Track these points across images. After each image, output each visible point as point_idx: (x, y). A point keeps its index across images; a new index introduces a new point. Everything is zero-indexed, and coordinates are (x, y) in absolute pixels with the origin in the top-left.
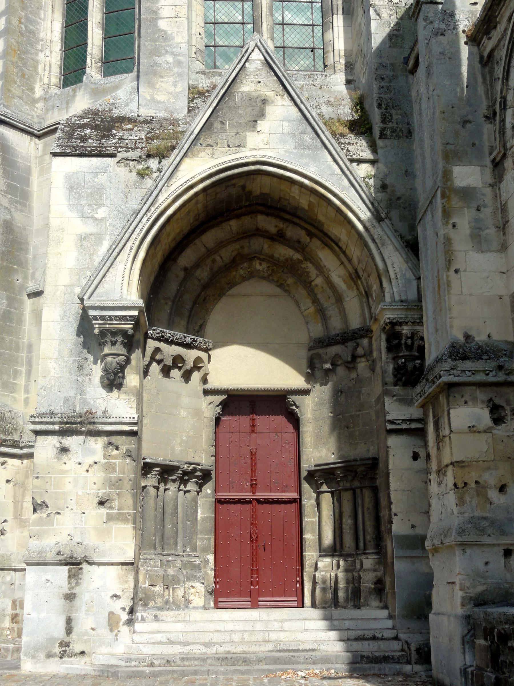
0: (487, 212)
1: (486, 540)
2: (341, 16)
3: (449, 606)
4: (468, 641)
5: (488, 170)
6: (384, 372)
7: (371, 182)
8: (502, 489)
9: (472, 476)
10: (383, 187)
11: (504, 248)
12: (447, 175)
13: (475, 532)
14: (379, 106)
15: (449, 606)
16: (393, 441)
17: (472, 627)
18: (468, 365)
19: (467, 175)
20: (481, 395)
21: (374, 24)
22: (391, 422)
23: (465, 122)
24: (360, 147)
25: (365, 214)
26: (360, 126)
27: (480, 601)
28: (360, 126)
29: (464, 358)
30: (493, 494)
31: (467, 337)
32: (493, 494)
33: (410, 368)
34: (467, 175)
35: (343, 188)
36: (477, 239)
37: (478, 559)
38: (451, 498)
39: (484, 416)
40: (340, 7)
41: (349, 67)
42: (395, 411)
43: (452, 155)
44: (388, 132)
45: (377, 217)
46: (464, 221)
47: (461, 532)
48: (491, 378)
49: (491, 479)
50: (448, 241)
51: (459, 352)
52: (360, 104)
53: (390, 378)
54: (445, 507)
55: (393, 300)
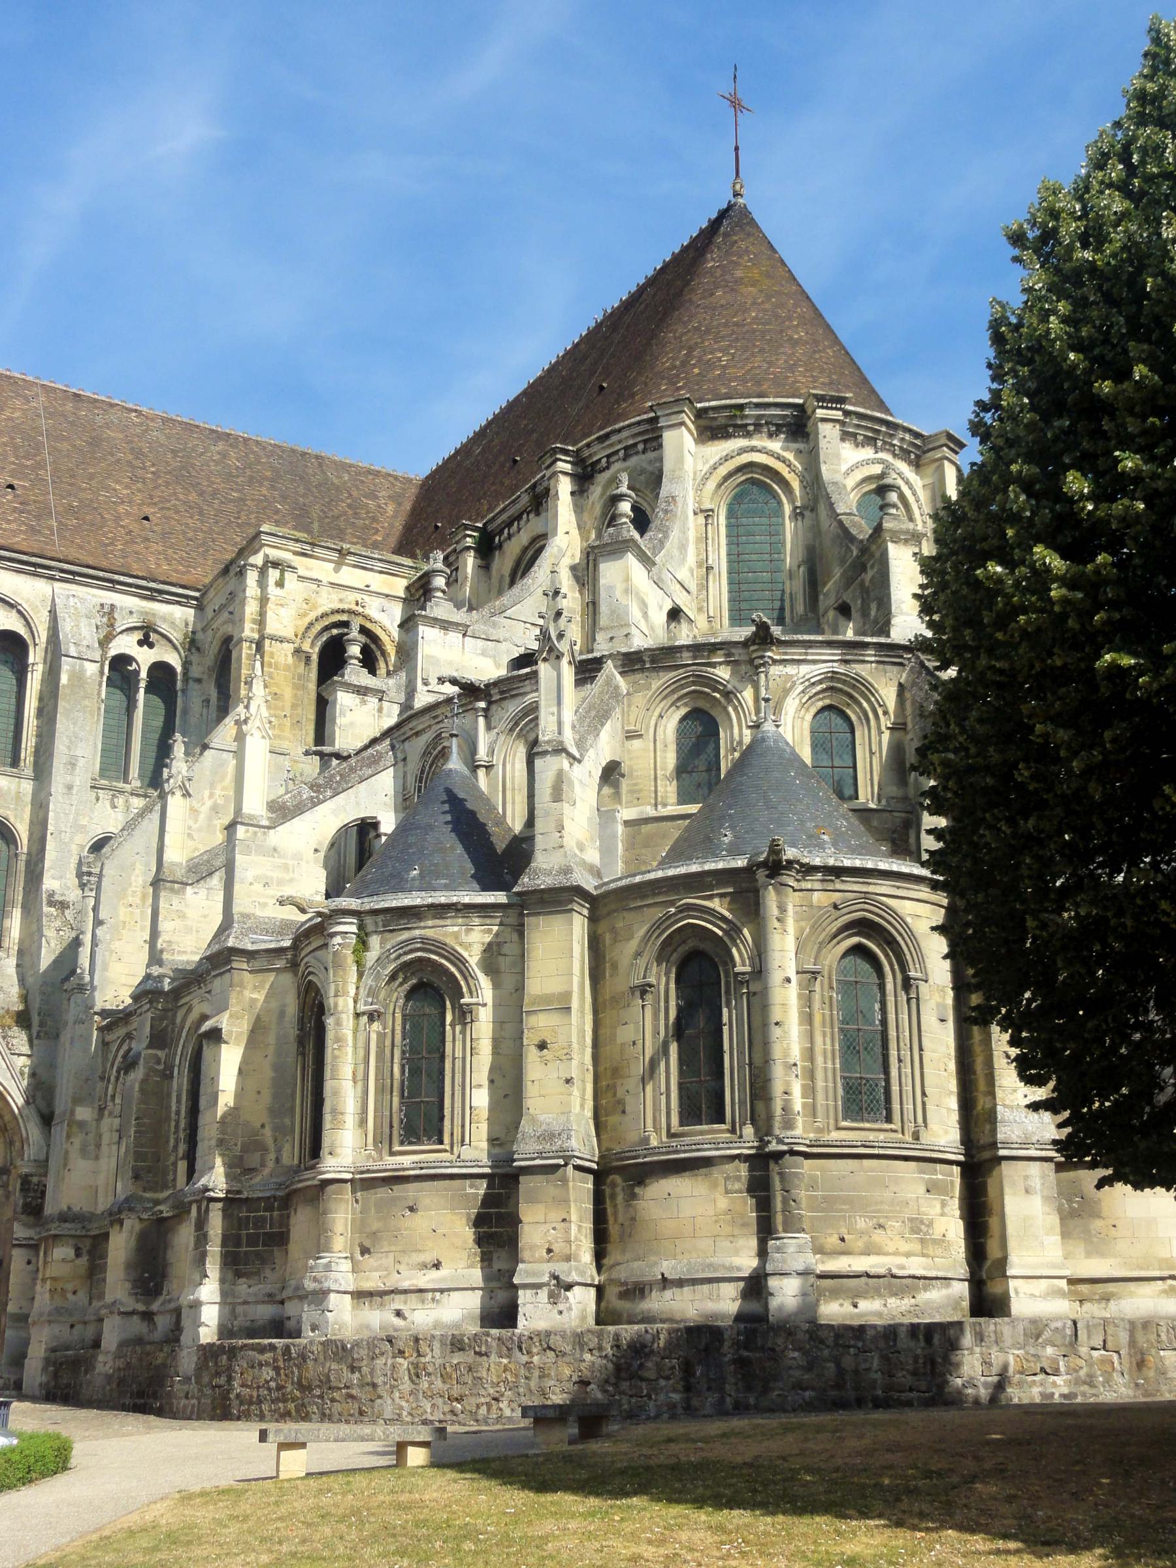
0: (91, 1136)
1: (61, 1319)
2: (19, 910)
3: (37, 1352)
4: (44, 1369)
5: (96, 1112)
6: (16, 1205)
7: (26, 1070)
8: (75, 1293)
9: (59, 1285)
10: (33, 1075)
11: (97, 1158)
12: (72, 1113)
13: (58, 1313)
14: (39, 1014)
15: (37, 1352)
16: (16, 1252)
17: (47, 1361)
18: (67, 1225)
19: (84, 1113)
20: (71, 1241)
21: (43, 950)
22: (17, 1239)
23: (87, 1080)
24: (20, 1040)
25: (21, 1101)
26: (23, 1019)
27: (54, 1350)
28: (23, 1019)
29: (65, 1221)
30: (70, 1296)
31: (69, 1208)
32: (70, 1296)
33: (34, 1209)
34: (84, 1113)
35: (7, 1079)
36: (83, 1152)
37: (56, 1329)
38: (47, 1296)
39: (71, 1252)
40: (20, 902)
41: (20, 953)
42: (20, 1232)
43: (77, 1100)
44: (42, 1034)
45: (27, 1102)
46: (77, 1141)
47: (50, 1314)
48: (78, 1233)
49: (70, 1287)
50: (67, 1152)
51: (64, 1218)
52: (25, 998)
53: (19, 1209)
54: (43, 1299)
55: (29, 1160)
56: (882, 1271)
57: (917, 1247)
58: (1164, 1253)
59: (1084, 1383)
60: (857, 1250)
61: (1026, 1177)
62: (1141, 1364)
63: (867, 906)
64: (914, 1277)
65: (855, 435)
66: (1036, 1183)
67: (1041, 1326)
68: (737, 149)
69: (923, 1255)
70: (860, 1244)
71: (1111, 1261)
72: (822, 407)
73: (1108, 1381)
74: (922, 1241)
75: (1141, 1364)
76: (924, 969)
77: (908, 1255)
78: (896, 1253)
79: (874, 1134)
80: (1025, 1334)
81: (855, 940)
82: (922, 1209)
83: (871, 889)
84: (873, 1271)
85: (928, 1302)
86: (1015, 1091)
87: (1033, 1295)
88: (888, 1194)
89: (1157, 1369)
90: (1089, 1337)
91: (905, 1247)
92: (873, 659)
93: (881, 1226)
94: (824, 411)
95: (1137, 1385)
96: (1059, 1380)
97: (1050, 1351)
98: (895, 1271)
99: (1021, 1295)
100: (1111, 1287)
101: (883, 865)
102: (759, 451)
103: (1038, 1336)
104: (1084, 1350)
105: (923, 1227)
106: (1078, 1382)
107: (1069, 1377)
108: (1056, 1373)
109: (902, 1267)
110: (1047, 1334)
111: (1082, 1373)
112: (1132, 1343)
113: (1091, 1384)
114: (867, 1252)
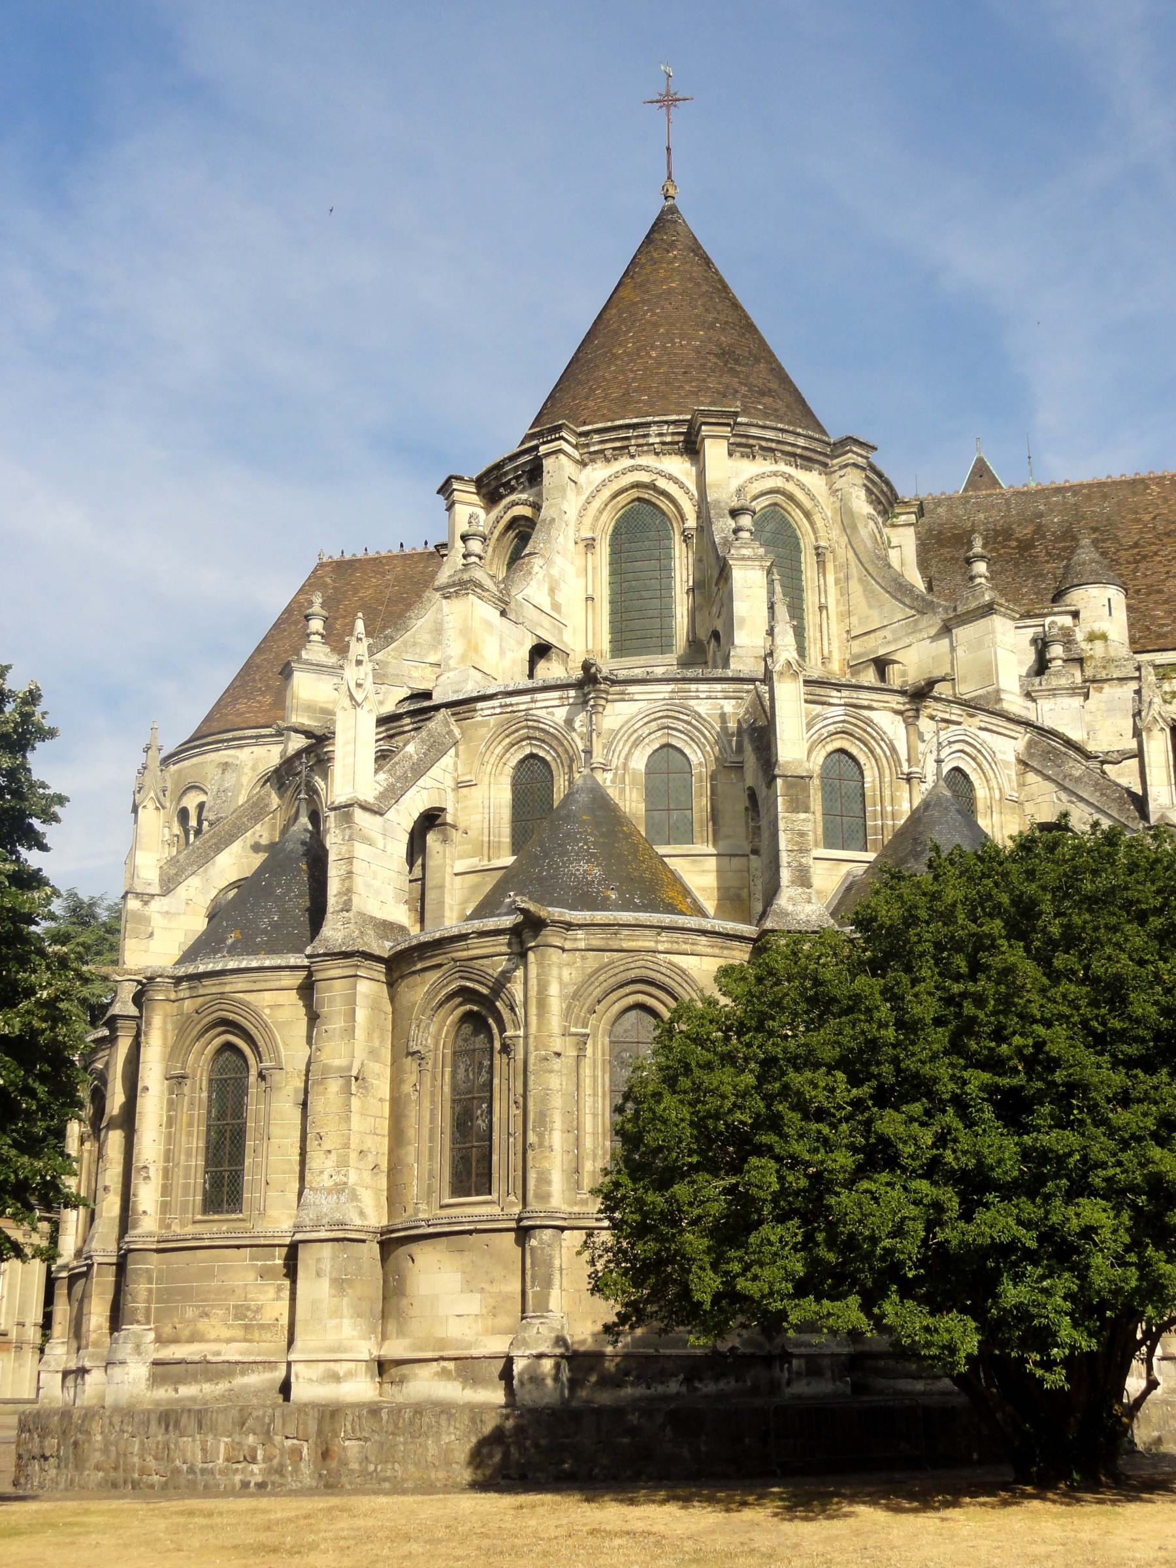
56: (197, 1358)
57: (240, 1333)
58: (440, 1333)
59: (276, 1472)
60: (183, 1338)
61: (319, 1260)
62: (325, 1455)
63: (223, 1006)
64: (228, 1362)
65: (602, 451)
66: (326, 1266)
67: (246, 1414)
68: (668, 149)
69: (246, 1340)
70: (187, 1333)
71: (406, 1342)
72: (544, 443)
73: (296, 1470)
74: (247, 1327)
75: (325, 1455)
76: (278, 1058)
77: (229, 1341)
78: (217, 1340)
79: (219, 1227)
80: (233, 1423)
81: (218, 1042)
82: (249, 1296)
83: (227, 989)
84: (190, 1358)
85: (245, 1387)
86: (322, 1172)
87: (310, 1380)
88: (215, 1283)
89: (340, 1459)
90: (284, 1425)
91: (226, 1333)
92: (410, 727)
93: (207, 1315)
94: (546, 446)
95: (320, 1475)
96: (255, 1468)
97: (251, 1439)
98: (209, 1358)
99: (301, 1380)
100: (405, 1369)
101: (232, 965)
102: (517, 504)
103: (243, 1424)
104: (278, 1439)
105: (249, 1313)
106: (270, 1471)
107: (264, 1466)
108: (254, 1461)
109: (218, 1354)
110: (249, 1423)
111: (276, 1462)
112: (320, 1432)
113: (282, 1475)
114: (191, 1340)
